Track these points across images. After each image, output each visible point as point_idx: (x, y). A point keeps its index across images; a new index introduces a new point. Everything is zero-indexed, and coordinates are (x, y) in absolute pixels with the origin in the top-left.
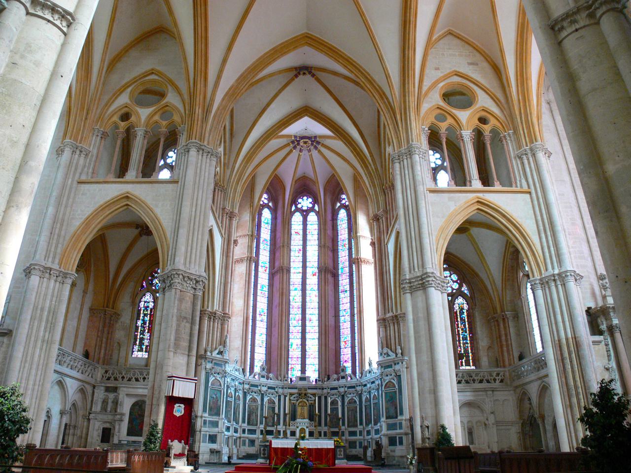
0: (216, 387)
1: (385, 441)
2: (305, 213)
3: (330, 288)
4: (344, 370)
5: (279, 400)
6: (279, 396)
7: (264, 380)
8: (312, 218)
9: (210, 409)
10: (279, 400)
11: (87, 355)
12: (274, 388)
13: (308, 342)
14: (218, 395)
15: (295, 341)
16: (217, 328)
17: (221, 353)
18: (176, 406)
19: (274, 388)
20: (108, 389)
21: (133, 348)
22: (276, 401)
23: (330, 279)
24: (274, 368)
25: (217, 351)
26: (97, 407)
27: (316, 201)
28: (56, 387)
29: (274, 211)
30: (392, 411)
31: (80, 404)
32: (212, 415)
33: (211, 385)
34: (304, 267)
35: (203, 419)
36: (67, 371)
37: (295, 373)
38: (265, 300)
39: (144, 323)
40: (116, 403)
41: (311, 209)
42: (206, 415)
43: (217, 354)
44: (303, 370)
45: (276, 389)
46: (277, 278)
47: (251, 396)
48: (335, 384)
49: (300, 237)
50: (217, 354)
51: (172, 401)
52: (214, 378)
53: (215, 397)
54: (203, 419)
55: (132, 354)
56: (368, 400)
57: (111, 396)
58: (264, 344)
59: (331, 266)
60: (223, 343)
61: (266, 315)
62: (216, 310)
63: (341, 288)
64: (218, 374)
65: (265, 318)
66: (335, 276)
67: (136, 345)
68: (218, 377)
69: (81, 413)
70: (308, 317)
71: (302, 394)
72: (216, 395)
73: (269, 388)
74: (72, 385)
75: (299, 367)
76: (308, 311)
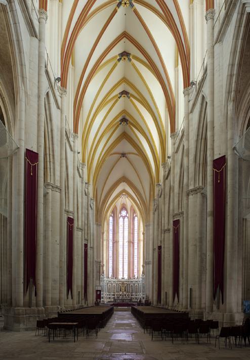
2: (124, 217)
3: (132, 248)
8: (126, 219)
13: (124, 266)
23: (131, 244)
24: (115, 276)
27: (127, 213)
29: (113, 217)
34: (123, 239)
37: (120, 277)
41: (126, 216)
44: (123, 275)
46: (115, 244)
49: (122, 227)
59: (132, 240)
65: (111, 258)
66: (133, 243)
71: (123, 283)
75: (122, 274)
76: (124, 255)
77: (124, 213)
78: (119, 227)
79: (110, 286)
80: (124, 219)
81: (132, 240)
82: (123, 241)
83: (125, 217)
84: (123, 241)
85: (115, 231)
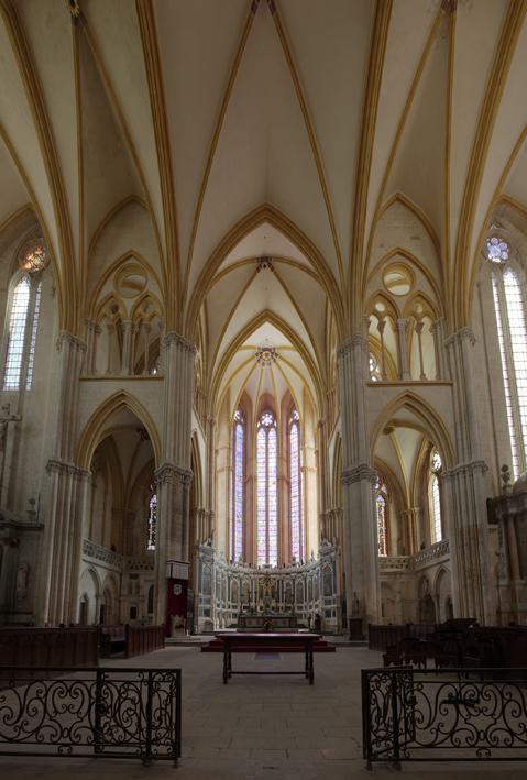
1: (322, 614)
4: (294, 559)
7: (241, 568)
11: (113, 549)
15: (261, 539)
17: (210, 544)
18: (175, 586)
20: (132, 577)
23: (285, 487)
26: (125, 592)
28: (89, 576)
30: (328, 591)
31: (111, 589)
34: (267, 477)
36: (97, 561)
37: (261, 563)
38: (241, 505)
40: (138, 587)
44: (267, 560)
48: (288, 570)
51: (172, 582)
56: (311, 582)
57: (134, 581)
60: (211, 536)
63: (293, 494)
66: (289, 484)
69: (113, 596)
70: (270, 518)
74: (102, 574)
75: (264, 558)
76: (270, 514)
77: (267, 420)
78: (256, 449)
79: (235, 583)
80: (267, 433)
81: (286, 475)
82: (267, 482)
83: (271, 426)
84: (267, 482)
85: (249, 455)
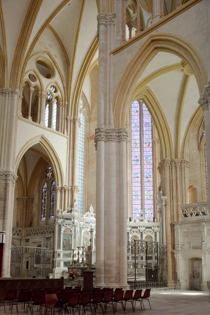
0: (68, 232)
5: (156, 235)
6: (156, 232)
9: (64, 247)
10: (156, 235)
12: (151, 228)
14: (70, 238)
16: (68, 196)
19: (151, 228)
21: (41, 216)
22: (153, 236)
25: (66, 211)
32: (66, 250)
33: (64, 232)
35: (57, 253)
39: (45, 201)
42: (61, 250)
43: (68, 212)
45: (153, 228)
47: (133, 235)
50: (68, 212)
52: (65, 228)
53: (67, 239)
54: (57, 253)
55: (41, 219)
58: (152, 198)
61: (152, 176)
62: (65, 186)
64: (69, 225)
67: (42, 214)
68: (68, 227)
72: (68, 238)
73: (147, 228)
